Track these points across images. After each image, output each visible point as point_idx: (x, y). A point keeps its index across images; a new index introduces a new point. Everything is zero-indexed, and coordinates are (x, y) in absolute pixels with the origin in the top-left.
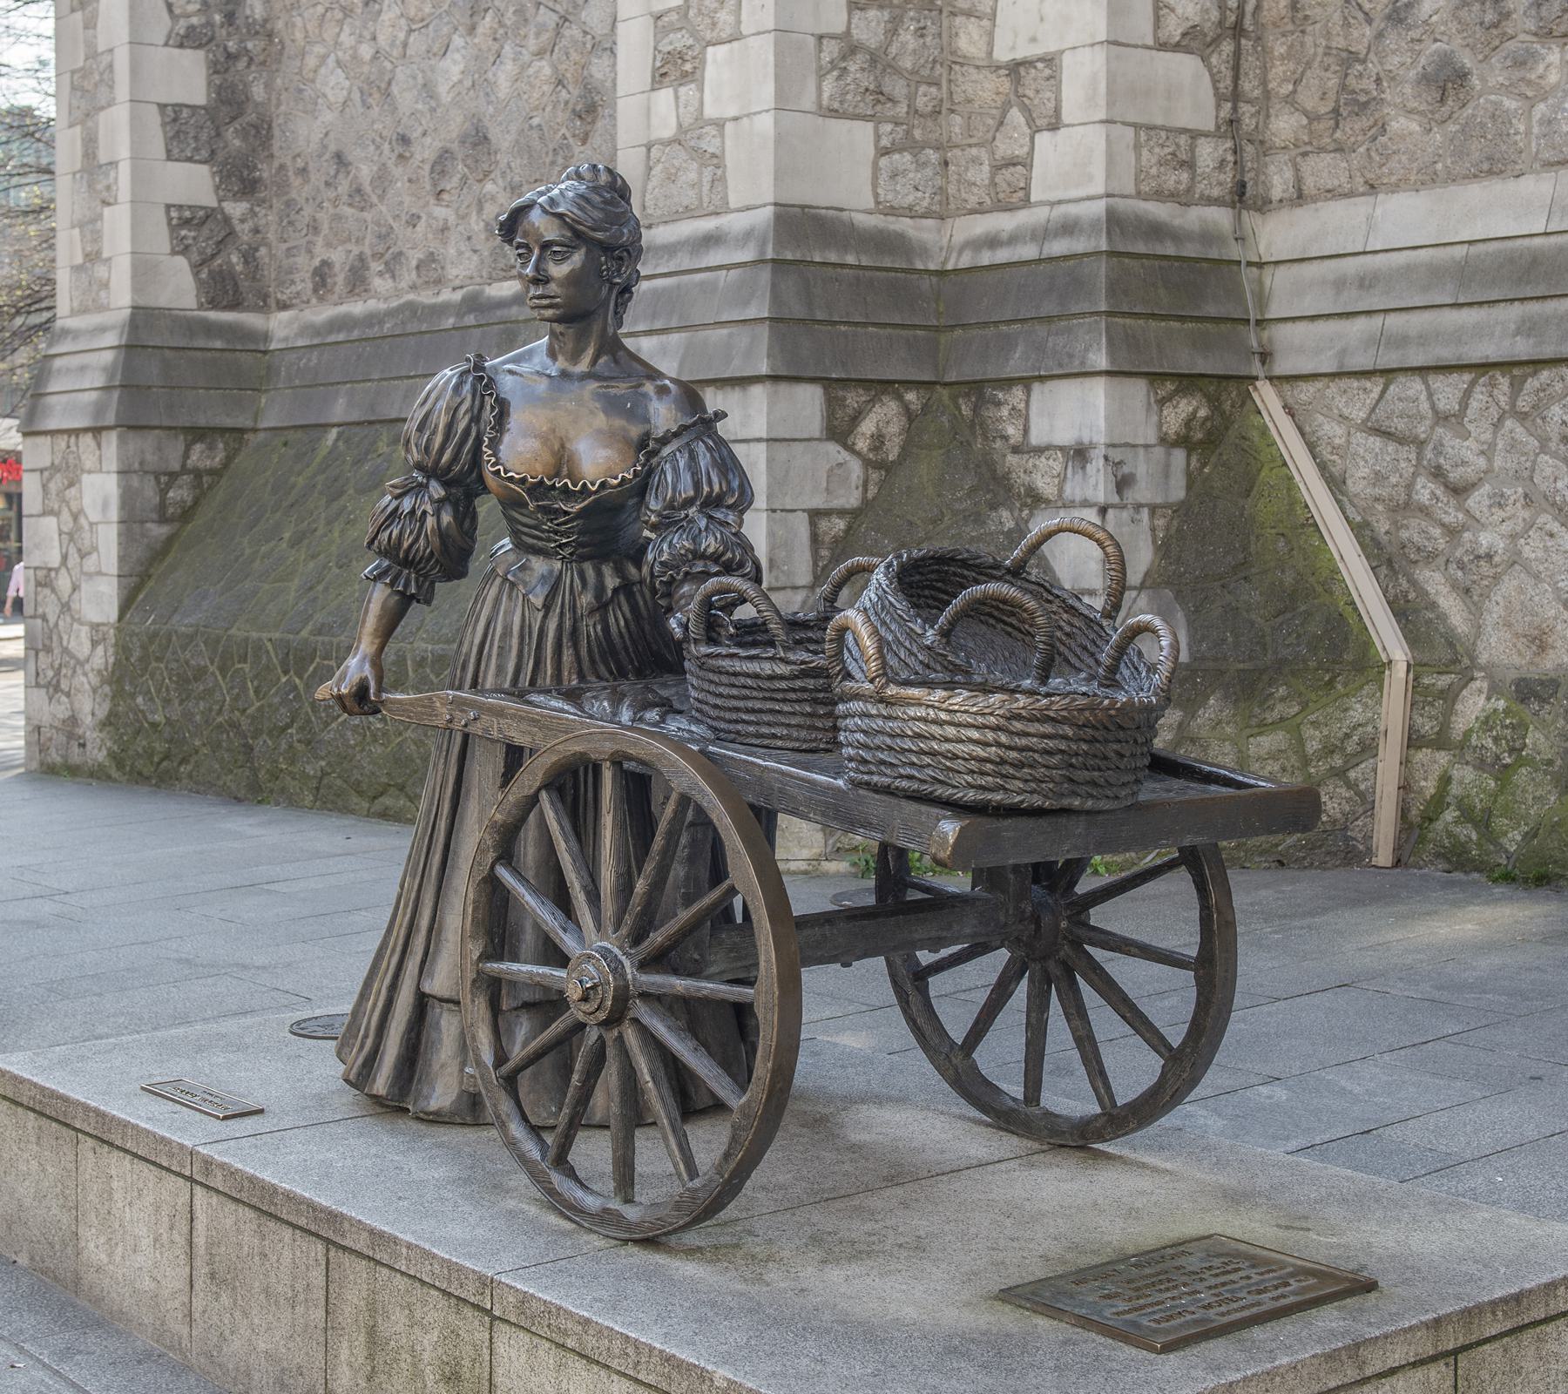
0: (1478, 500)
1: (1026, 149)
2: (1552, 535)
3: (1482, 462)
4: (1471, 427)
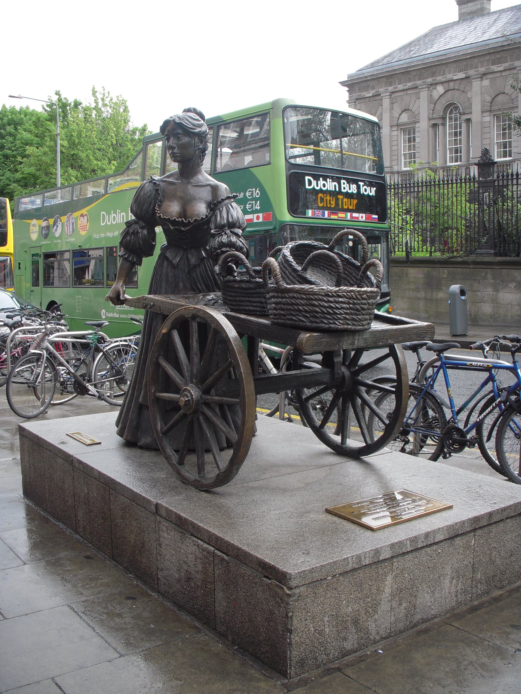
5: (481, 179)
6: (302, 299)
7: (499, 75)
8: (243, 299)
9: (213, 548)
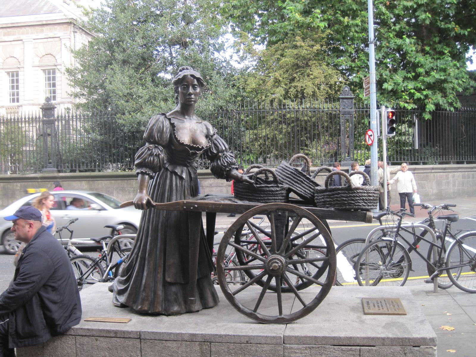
5: (44, 119)
6: (365, 193)
7: (9, 43)
8: (270, 198)
9: (359, 347)
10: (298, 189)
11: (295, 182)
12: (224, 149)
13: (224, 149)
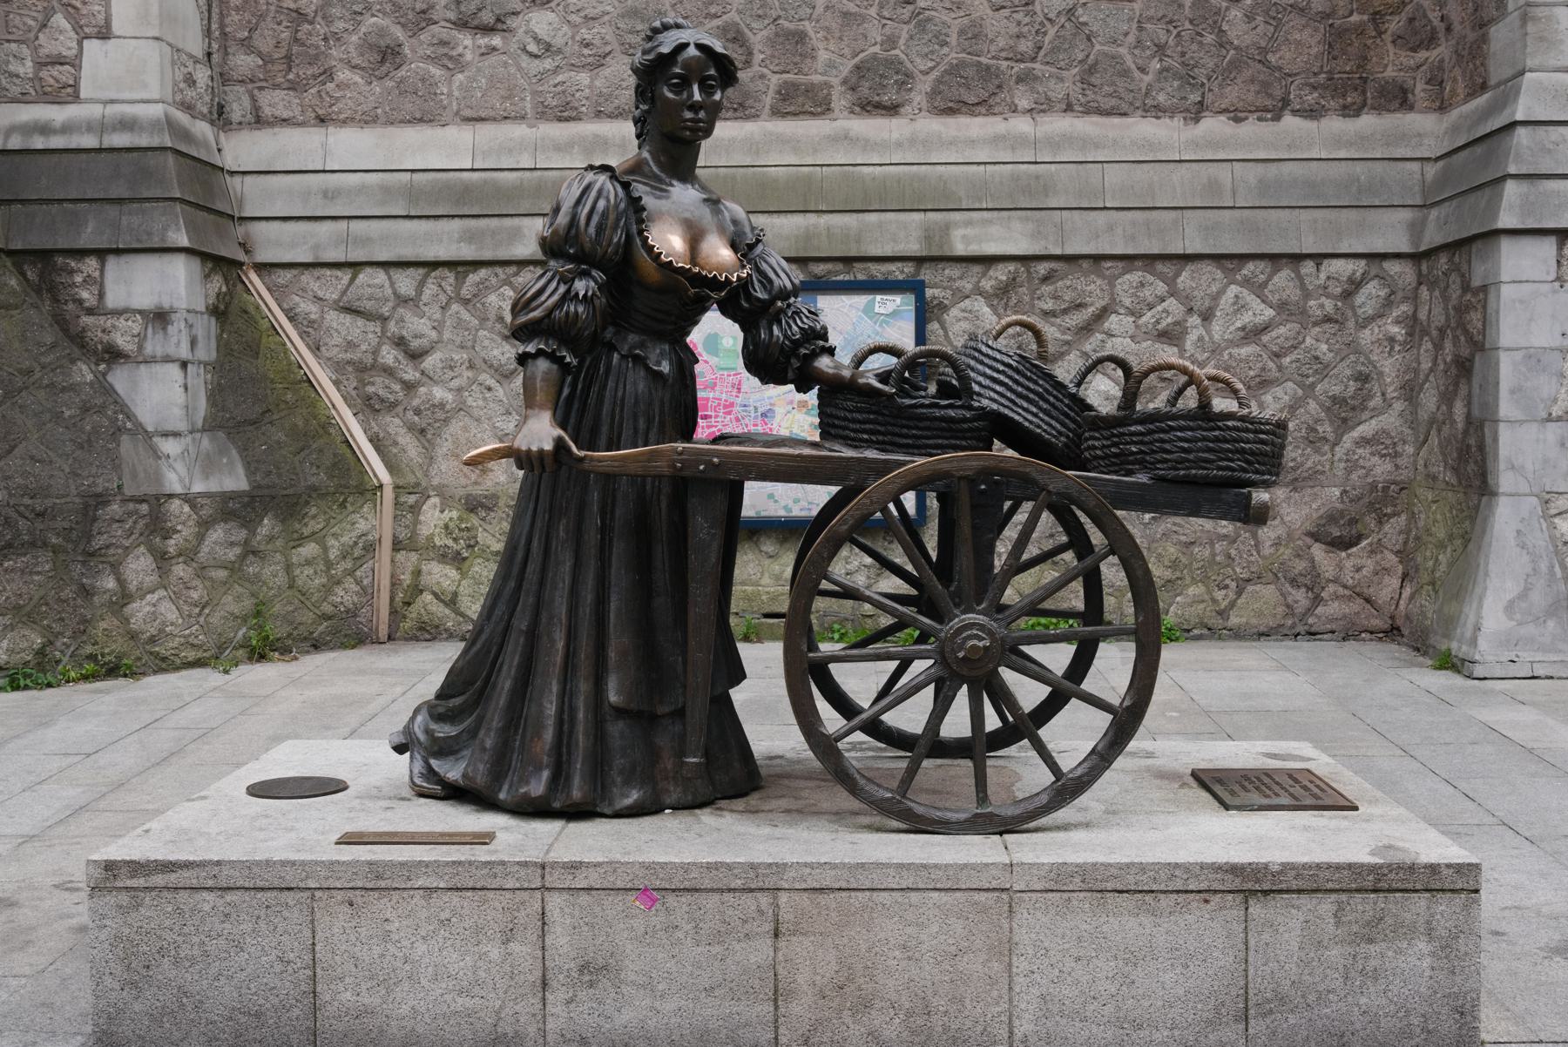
0: (430, 362)
1: (74, 52)
2: (489, 389)
3: (434, 334)
4: (426, 309)
6: (1247, 430)
10: (1030, 417)
11: (1019, 395)
12: (789, 285)
13: (789, 285)
